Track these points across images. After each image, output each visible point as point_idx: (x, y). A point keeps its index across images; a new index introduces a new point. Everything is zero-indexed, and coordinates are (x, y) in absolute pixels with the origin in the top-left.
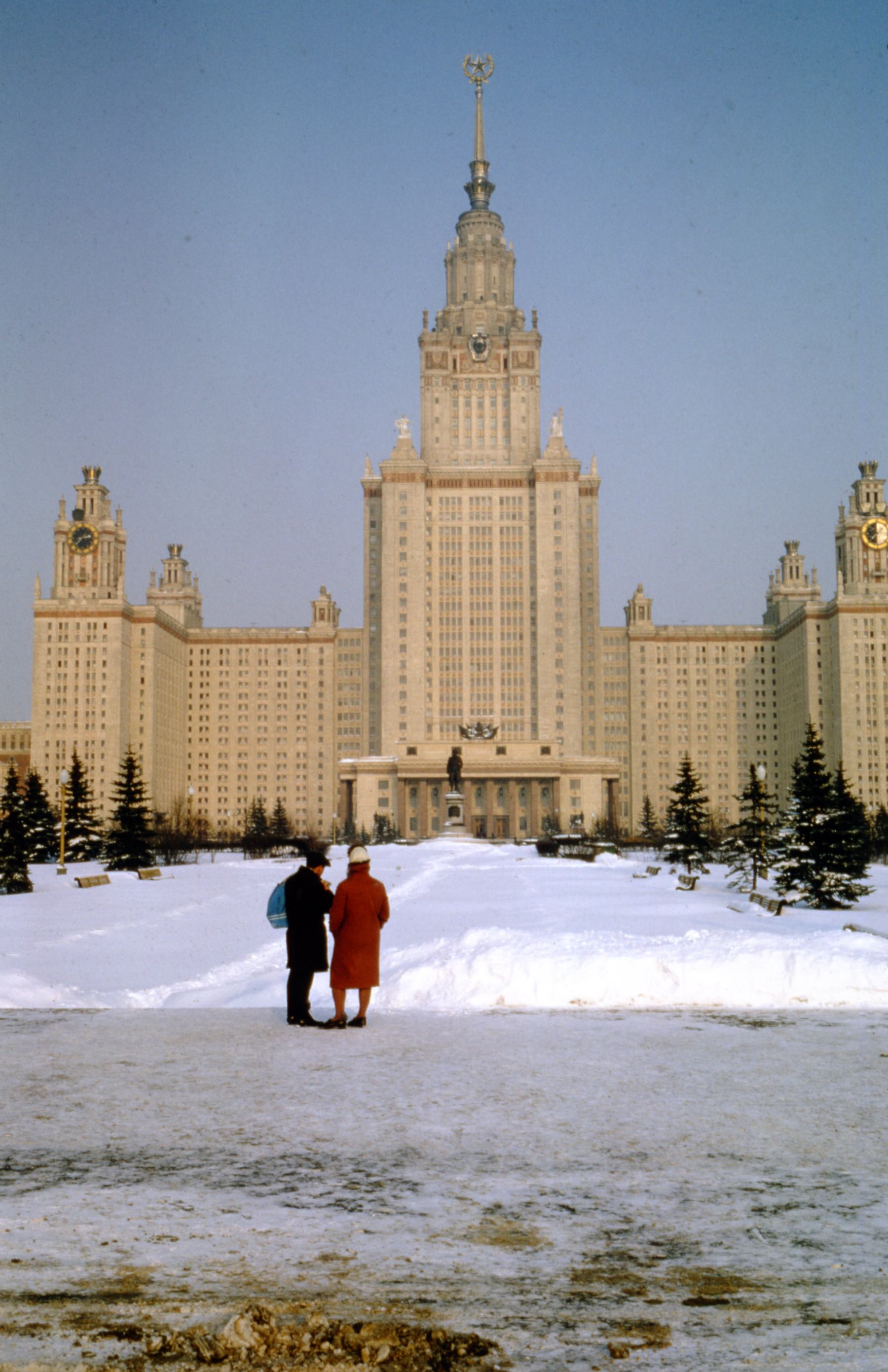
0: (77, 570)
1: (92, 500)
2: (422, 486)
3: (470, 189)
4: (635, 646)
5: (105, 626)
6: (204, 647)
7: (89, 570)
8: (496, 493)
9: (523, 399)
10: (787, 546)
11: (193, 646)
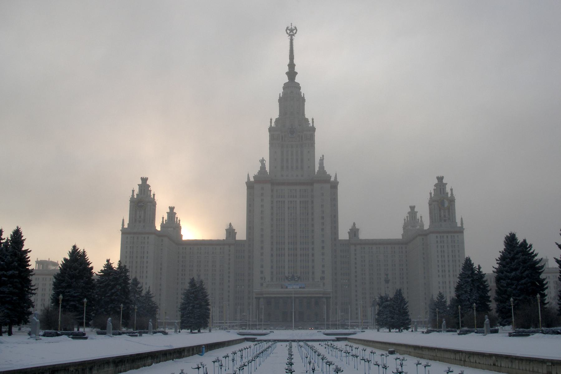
1: (144, 190)
5: (148, 237)
9: (309, 151)
10: (411, 207)
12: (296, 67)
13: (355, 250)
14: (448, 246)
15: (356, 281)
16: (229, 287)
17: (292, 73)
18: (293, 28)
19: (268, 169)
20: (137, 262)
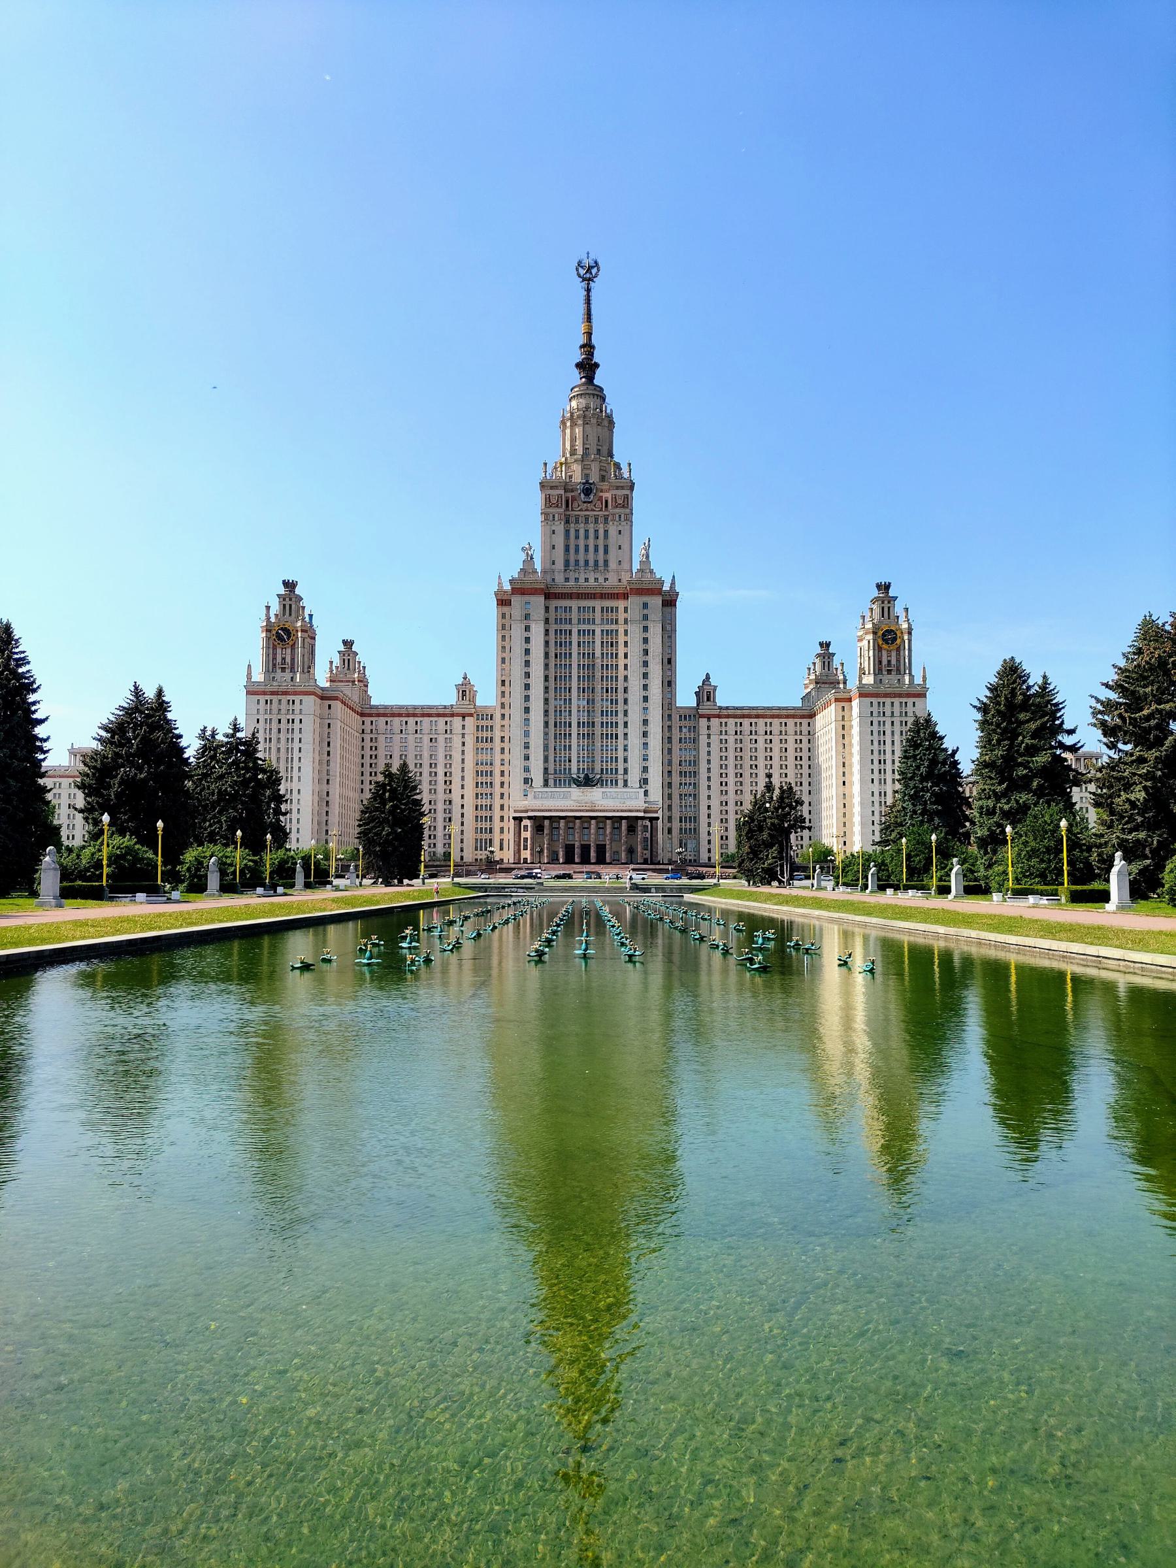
0: (279, 659)
1: (290, 605)
2: (542, 598)
3: (579, 366)
4: (703, 722)
6: (374, 719)
7: (288, 660)
8: (598, 604)
11: (364, 719)
12: (595, 353)
13: (709, 728)
14: (893, 722)
16: (462, 797)
17: (588, 367)
19: (538, 566)
20: (279, 749)
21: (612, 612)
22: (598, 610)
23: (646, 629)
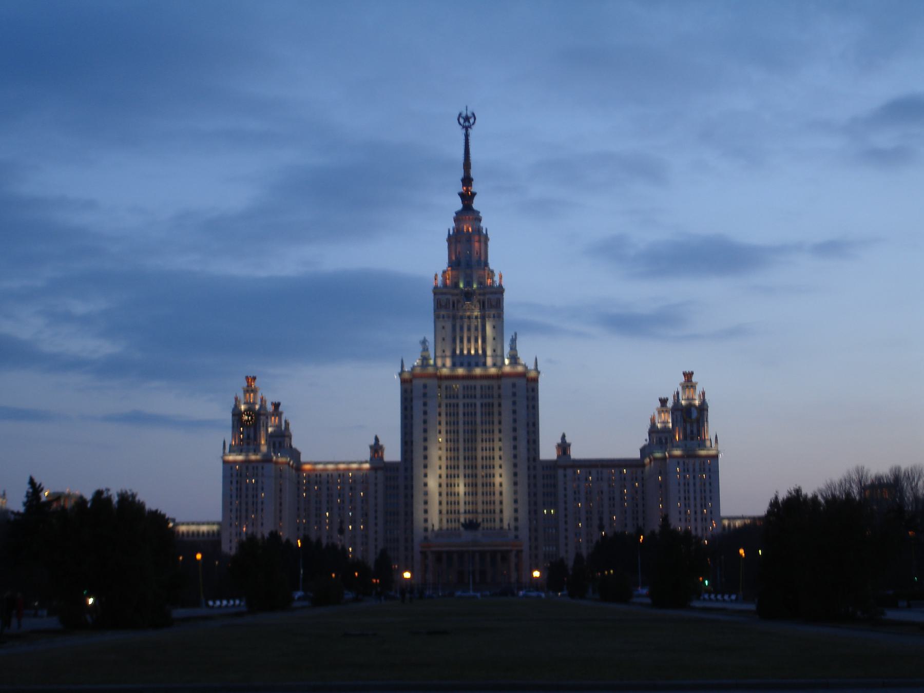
5: (263, 468)
13: (565, 476)
15: (566, 522)
16: (376, 532)
17: (467, 198)
18: (469, 114)
21: (489, 388)
22: (478, 388)
23: (514, 403)
